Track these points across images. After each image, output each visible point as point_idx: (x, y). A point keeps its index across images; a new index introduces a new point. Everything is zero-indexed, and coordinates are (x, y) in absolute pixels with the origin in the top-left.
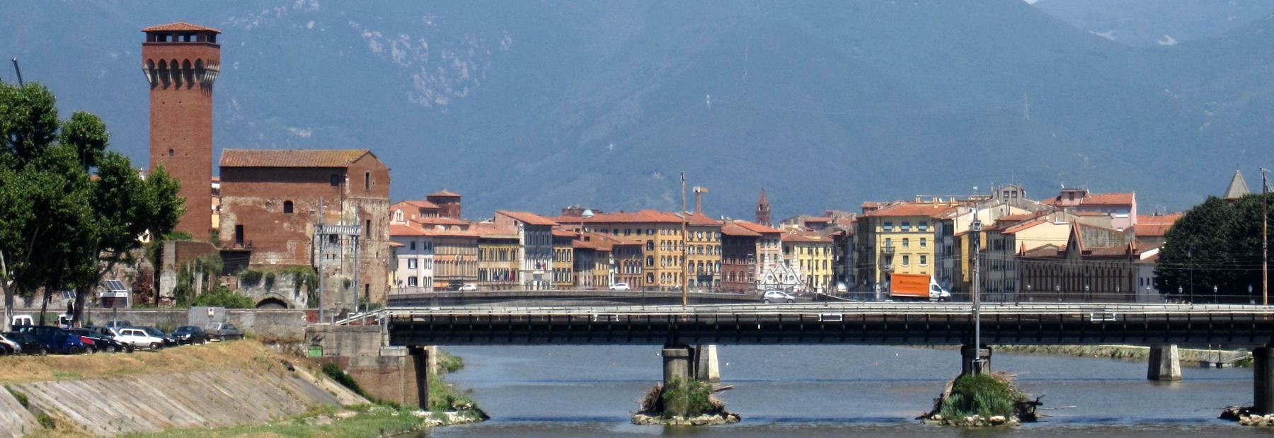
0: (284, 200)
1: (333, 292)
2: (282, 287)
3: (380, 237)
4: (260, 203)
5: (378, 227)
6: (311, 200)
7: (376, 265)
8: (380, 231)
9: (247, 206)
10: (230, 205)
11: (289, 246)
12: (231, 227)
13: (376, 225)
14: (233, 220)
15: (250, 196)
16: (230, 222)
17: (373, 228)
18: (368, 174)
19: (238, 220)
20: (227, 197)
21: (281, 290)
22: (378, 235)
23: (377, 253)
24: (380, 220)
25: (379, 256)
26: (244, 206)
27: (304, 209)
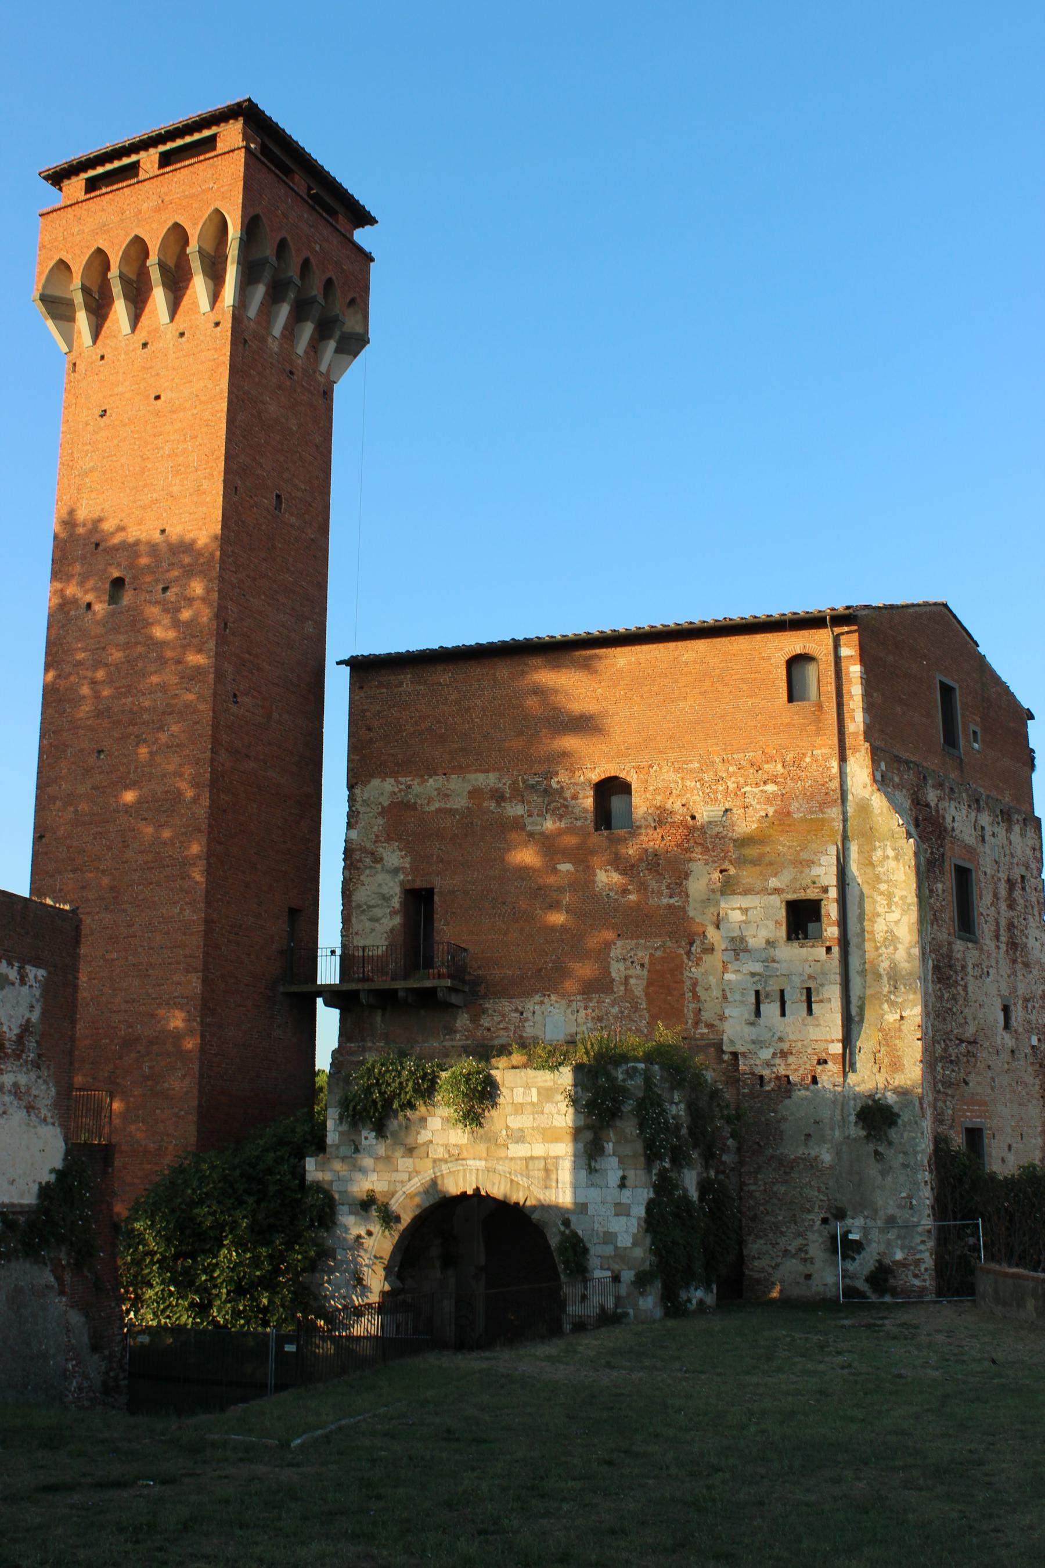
0: (595, 777)
1: (812, 1164)
2: (520, 1138)
3: (1013, 945)
4: (499, 797)
5: (1003, 906)
6: (708, 764)
7: (1005, 1056)
8: (1011, 926)
9: (451, 812)
10: (384, 812)
11: (617, 970)
12: (386, 898)
13: (996, 896)
14: (396, 871)
15: (461, 770)
16: (381, 877)
17: (983, 904)
18: (947, 691)
19: (414, 869)
20: (375, 782)
21: (517, 1150)
23: (1006, 1009)
24: (1011, 883)
25: (1014, 1023)
26: (439, 810)
27: (677, 806)
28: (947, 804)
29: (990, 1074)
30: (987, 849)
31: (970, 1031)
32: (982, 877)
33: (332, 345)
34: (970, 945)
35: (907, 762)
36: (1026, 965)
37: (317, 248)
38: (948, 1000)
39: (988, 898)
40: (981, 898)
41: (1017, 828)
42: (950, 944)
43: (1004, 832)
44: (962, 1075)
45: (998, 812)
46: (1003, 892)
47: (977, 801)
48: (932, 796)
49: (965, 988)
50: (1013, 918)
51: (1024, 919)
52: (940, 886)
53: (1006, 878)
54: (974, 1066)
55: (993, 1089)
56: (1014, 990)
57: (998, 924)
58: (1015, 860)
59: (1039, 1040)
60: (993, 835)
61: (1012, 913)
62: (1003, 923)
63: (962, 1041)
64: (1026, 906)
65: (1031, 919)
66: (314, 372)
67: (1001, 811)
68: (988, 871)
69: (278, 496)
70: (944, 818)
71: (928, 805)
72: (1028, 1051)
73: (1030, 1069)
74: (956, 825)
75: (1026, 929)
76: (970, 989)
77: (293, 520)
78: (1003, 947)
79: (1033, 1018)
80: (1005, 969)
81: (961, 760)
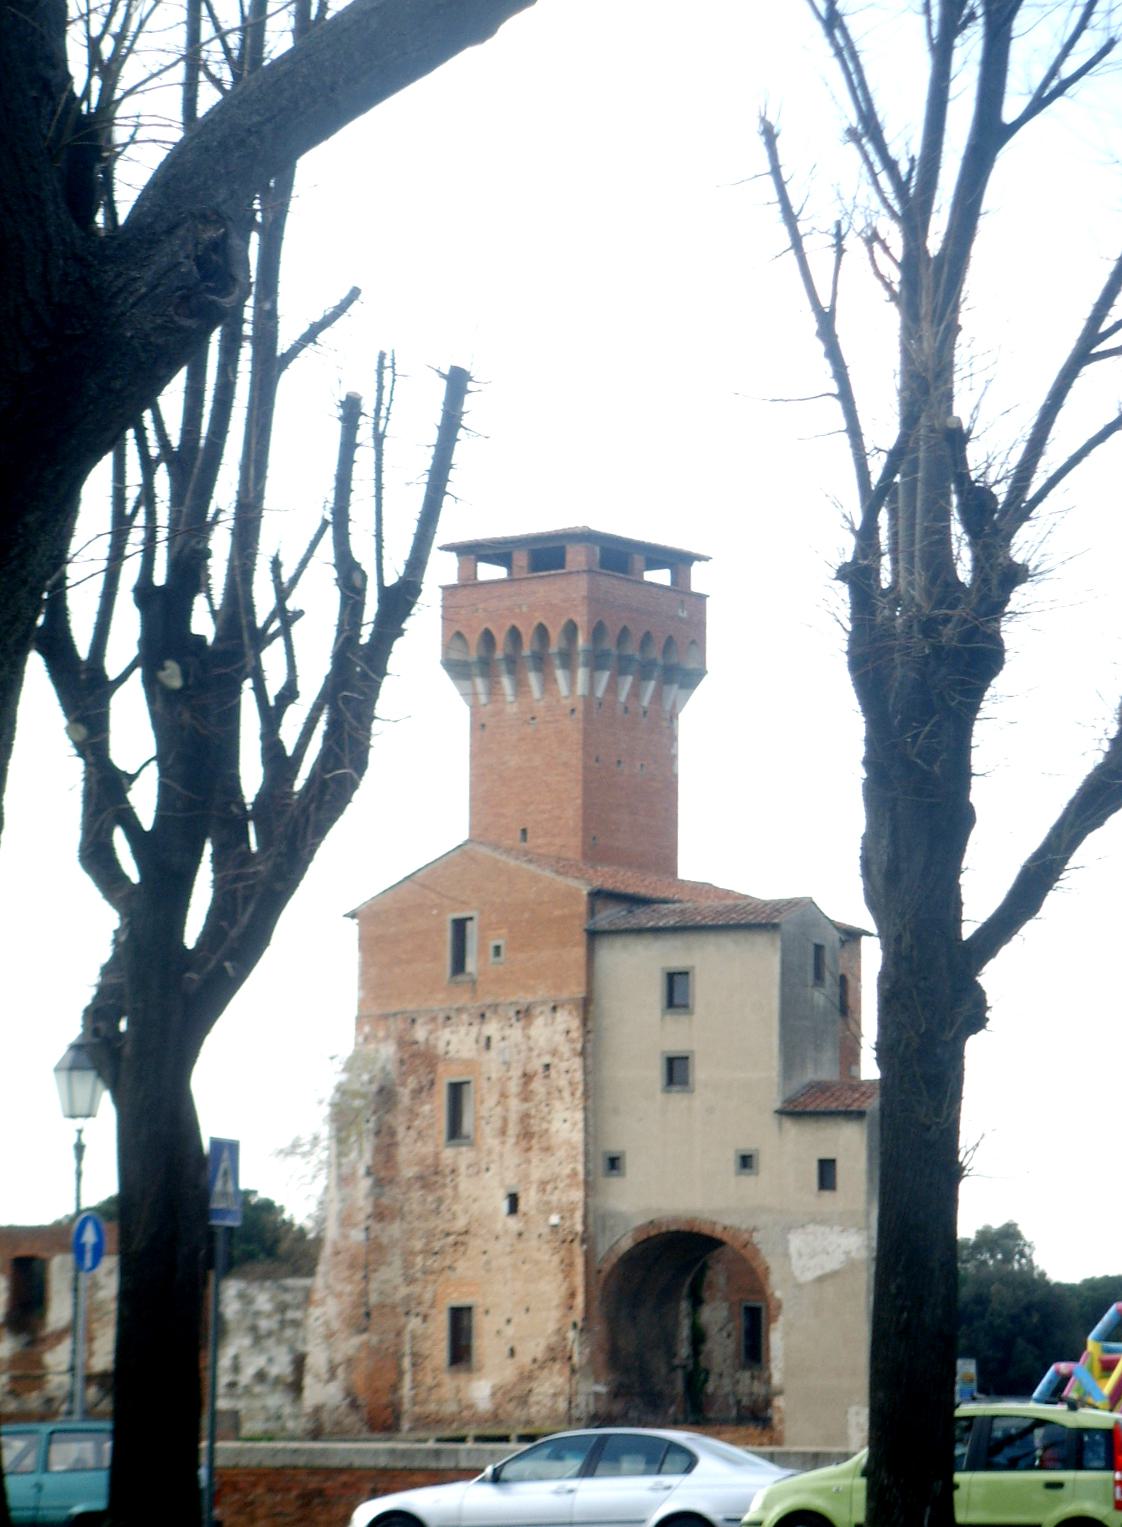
3: (527, 1135)
8: (525, 1117)
13: (504, 1095)
22: (513, 1129)
24: (527, 1078)
25: (522, 1206)
28: (439, 1033)
29: (485, 1258)
30: (493, 1053)
31: (460, 1224)
32: (485, 1084)
33: (560, 675)
34: (464, 1149)
35: (395, 1015)
36: (547, 1149)
37: (525, 609)
38: (432, 1203)
39: (491, 1100)
40: (482, 1102)
41: (539, 1022)
42: (437, 1155)
43: (520, 1031)
44: (447, 1262)
45: (512, 1013)
46: (514, 1087)
47: (483, 1016)
48: (420, 1033)
49: (455, 1188)
50: (528, 1109)
51: (547, 1105)
52: (427, 1108)
53: (519, 1073)
54: (464, 1253)
55: (488, 1271)
56: (525, 1178)
57: (505, 1120)
58: (535, 1053)
59: (562, 1218)
60: (503, 1039)
61: (526, 1105)
62: (513, 1117)
63: (448, 1234)
64: (549, 1093)
65: (557, 1105)
66: (558, 701)
67: (518, 1012)
68: (494, 1076)
69: (524, 831)
70: (435, 1047)
71: (416, 1043)
72: (545, 1231)
73: (545, 1247)
74: (450, 1048)
75: (549, 1113)
76: (462, 1187)
77: (540, 841)
78: (511, 1140)
79: (554, 1198)
80: (512, 1158)
81: (474, 982)
